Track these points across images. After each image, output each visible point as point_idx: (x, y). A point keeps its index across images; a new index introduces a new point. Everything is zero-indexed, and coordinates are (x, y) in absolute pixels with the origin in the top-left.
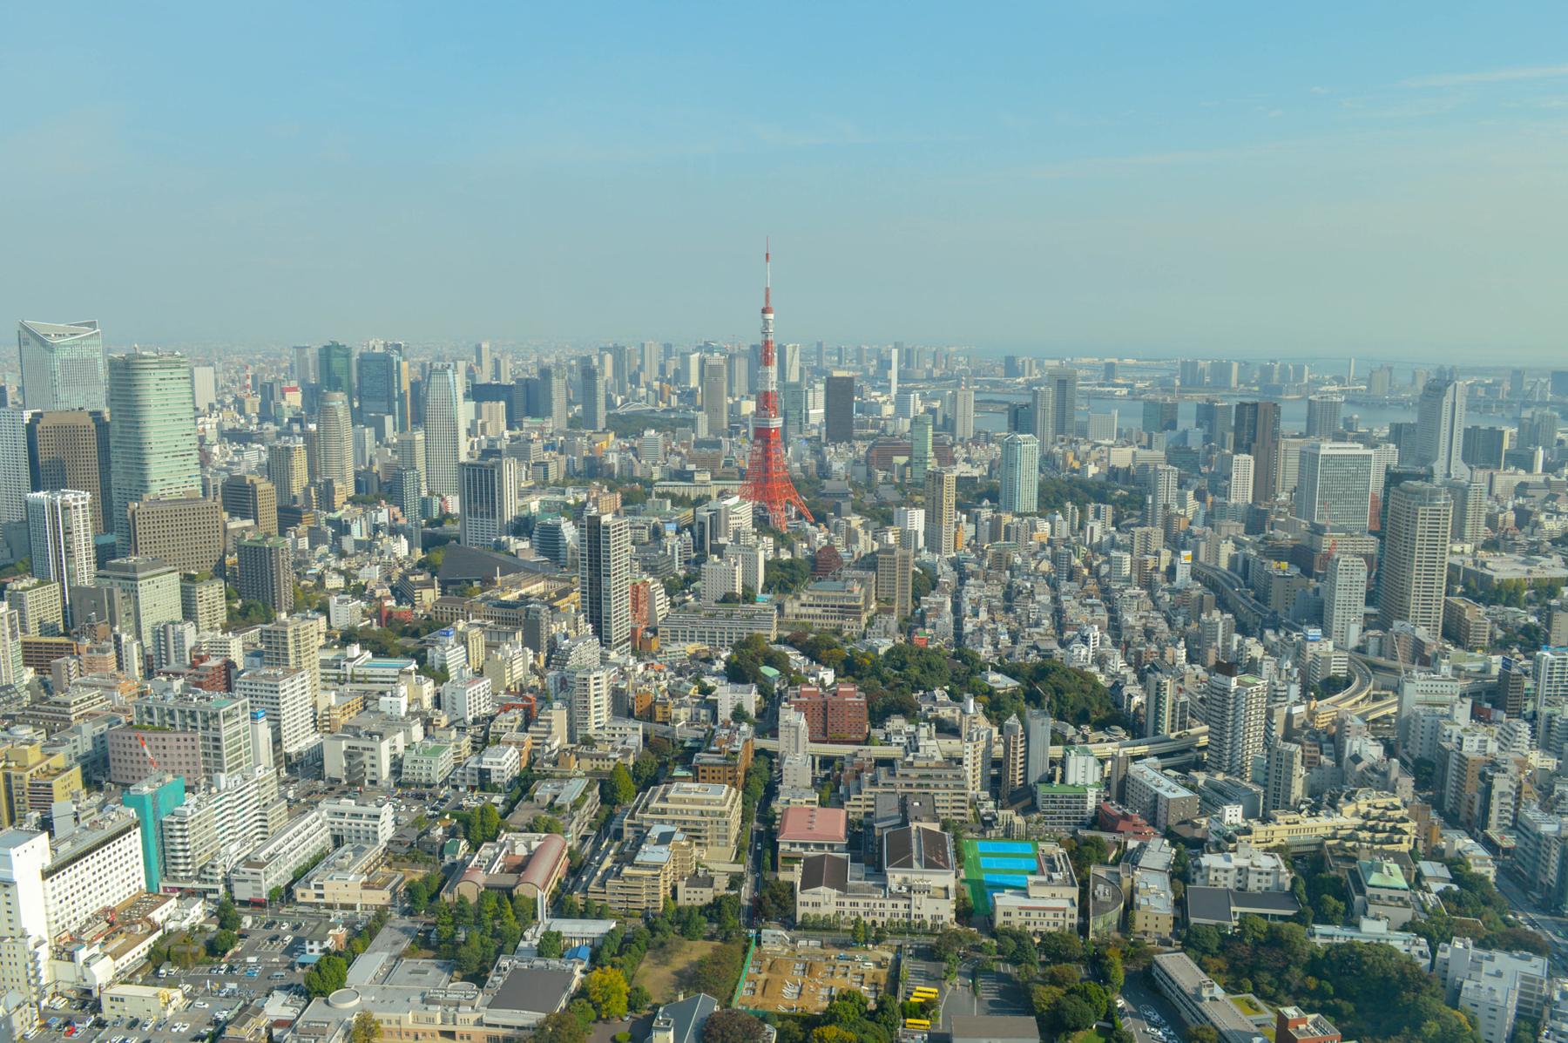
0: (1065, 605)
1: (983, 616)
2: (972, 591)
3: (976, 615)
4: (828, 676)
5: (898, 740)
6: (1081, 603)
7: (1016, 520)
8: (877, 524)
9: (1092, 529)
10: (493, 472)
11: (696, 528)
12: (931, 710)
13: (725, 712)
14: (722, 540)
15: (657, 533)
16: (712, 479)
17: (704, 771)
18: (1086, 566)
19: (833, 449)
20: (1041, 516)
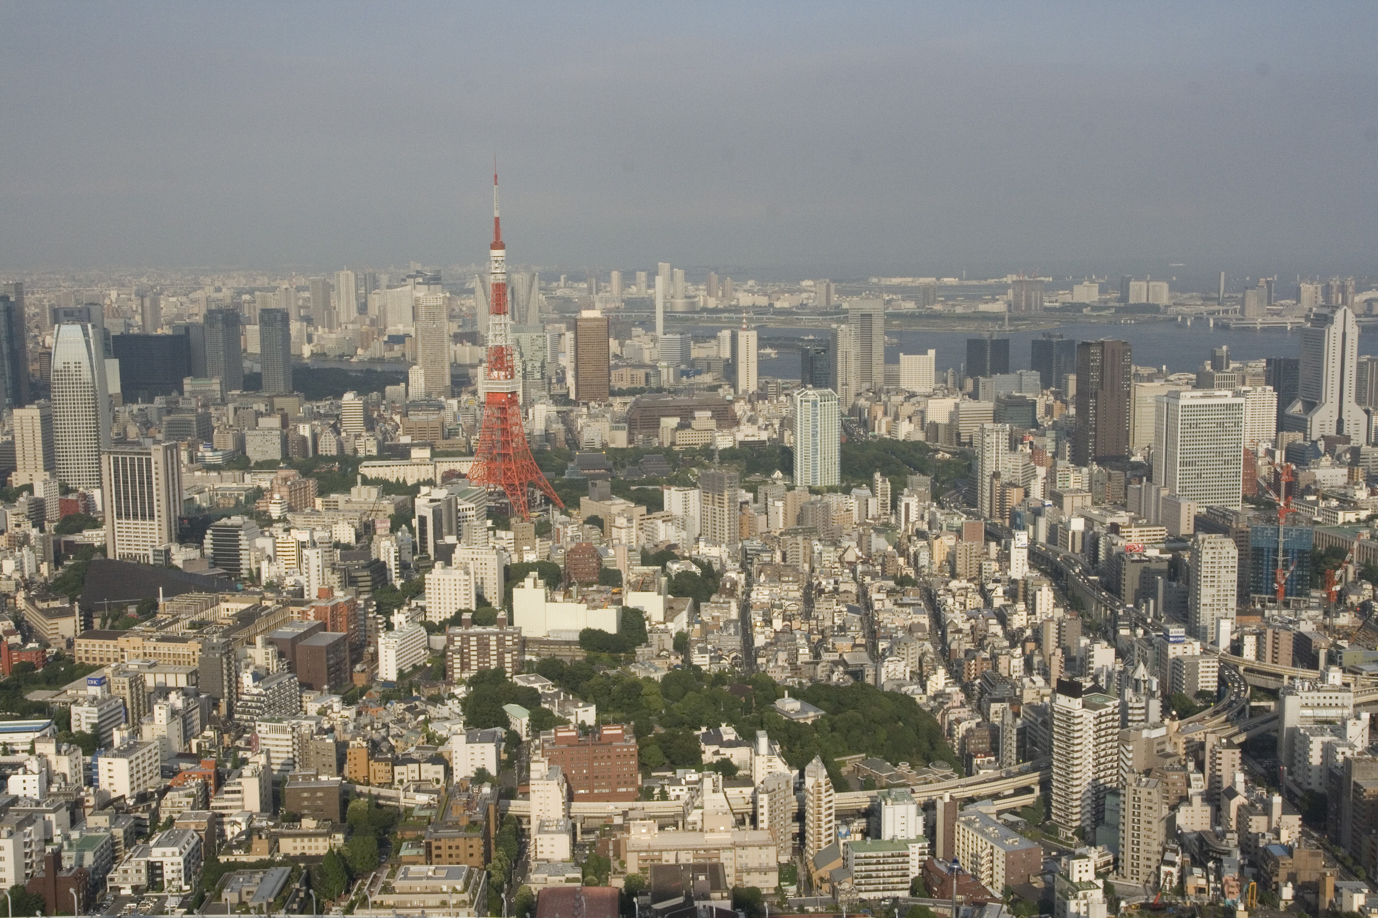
0: (877, 605)
1: (778, 624)
2: (761, 595)
3: (768, 622)
4: (588, 714)
5: (678, 792)
6: (896, 603)
7: (814, 498)
8: (643, 509)
9: (907, 505)
10: (149, 461)
11: (415, 522)
12: (716, 753)
13: (463, 769)
14: (450, 539)
15: (366, 531)
16: (434, 455)
17: (438, 848)
18: (902, 554)
19: (585, 410)
20: (847, 491)
